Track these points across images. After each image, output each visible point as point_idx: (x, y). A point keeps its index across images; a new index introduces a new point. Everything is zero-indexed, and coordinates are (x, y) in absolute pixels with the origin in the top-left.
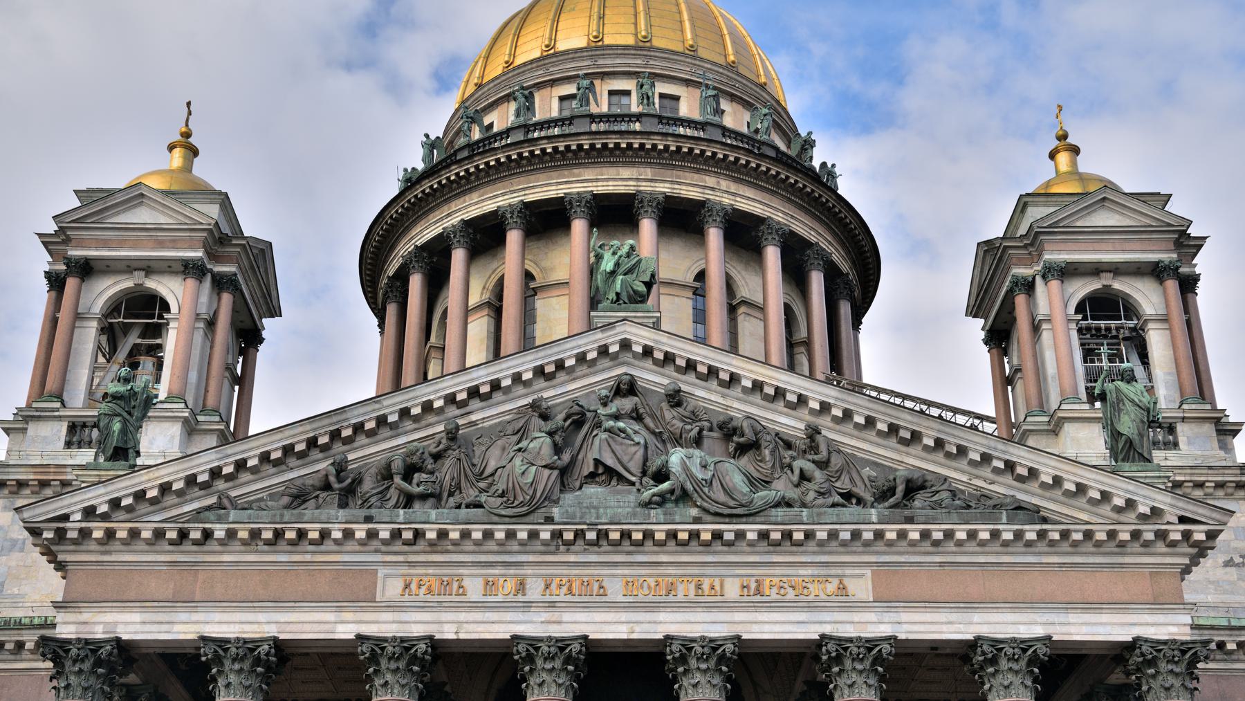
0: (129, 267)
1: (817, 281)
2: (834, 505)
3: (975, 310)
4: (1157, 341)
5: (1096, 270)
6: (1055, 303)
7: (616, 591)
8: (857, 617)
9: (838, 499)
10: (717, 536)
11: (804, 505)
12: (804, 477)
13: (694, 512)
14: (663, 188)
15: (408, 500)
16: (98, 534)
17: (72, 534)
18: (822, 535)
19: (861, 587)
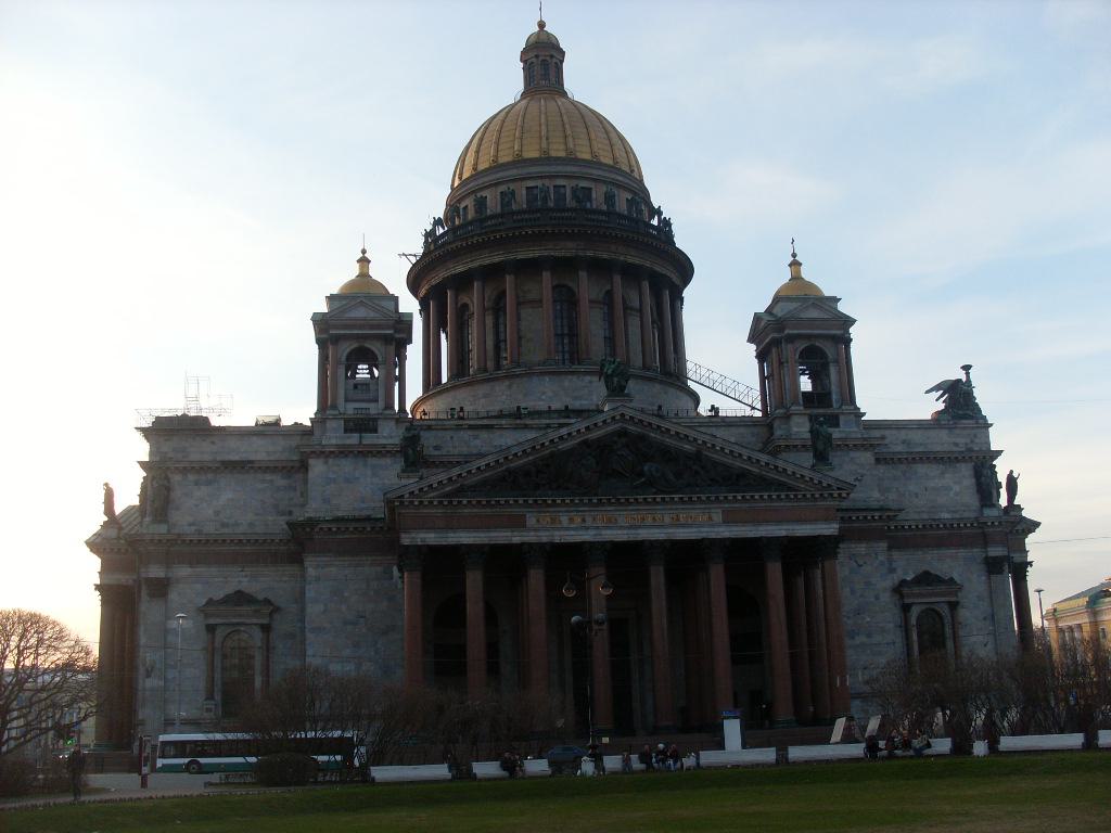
0: (357, 337)
2: (709, 485)
3: (751, 340)
4: (833, 370)
5: (809, 337)
6: (791, 351)
7: (621, 521)
8: (716, 530)
9: (709, 482)
10: (663, 499)
11: (697, 486)
12: (697, 472)
13: (654, 490)
14: (590, 253)
16: (416, 503)
17: (406, 503)
18: (704, 498)
19: (717, 516)
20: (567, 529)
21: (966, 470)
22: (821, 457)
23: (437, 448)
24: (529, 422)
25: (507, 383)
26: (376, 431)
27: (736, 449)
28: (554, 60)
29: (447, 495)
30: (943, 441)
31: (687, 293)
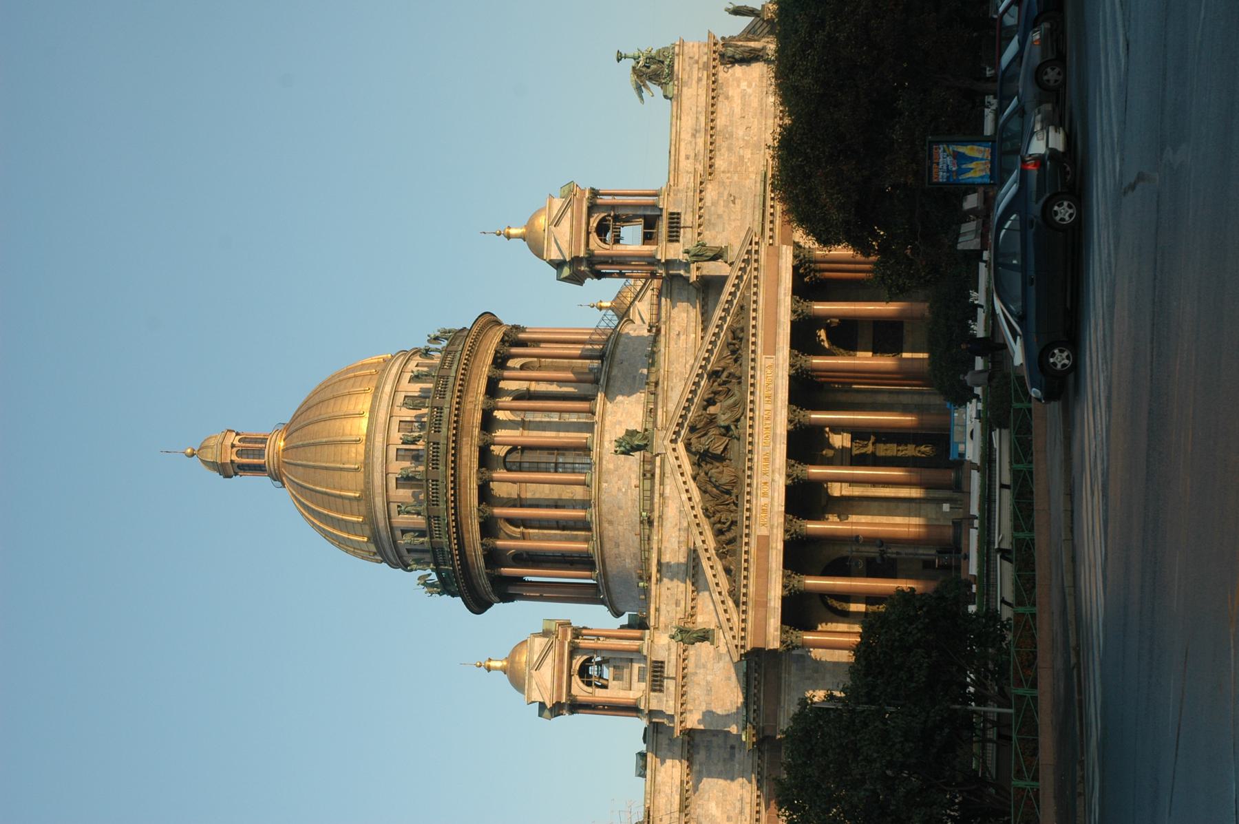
0: (570, 676)
1: (514, 350)
5: (588, 233)
8: (781, 362)
14: (476, 431)
15: (734, 523)
20: (772, 498)
21: (724, 74)
22: (717, 256)
23: (677, 604)
24: (656, 514)
25: (606, 525)
26: (662, 662)
27: (709, 337)
28: (236, 442)
29: (737, 604)
30: (694, 94)
31: (508, 320)
